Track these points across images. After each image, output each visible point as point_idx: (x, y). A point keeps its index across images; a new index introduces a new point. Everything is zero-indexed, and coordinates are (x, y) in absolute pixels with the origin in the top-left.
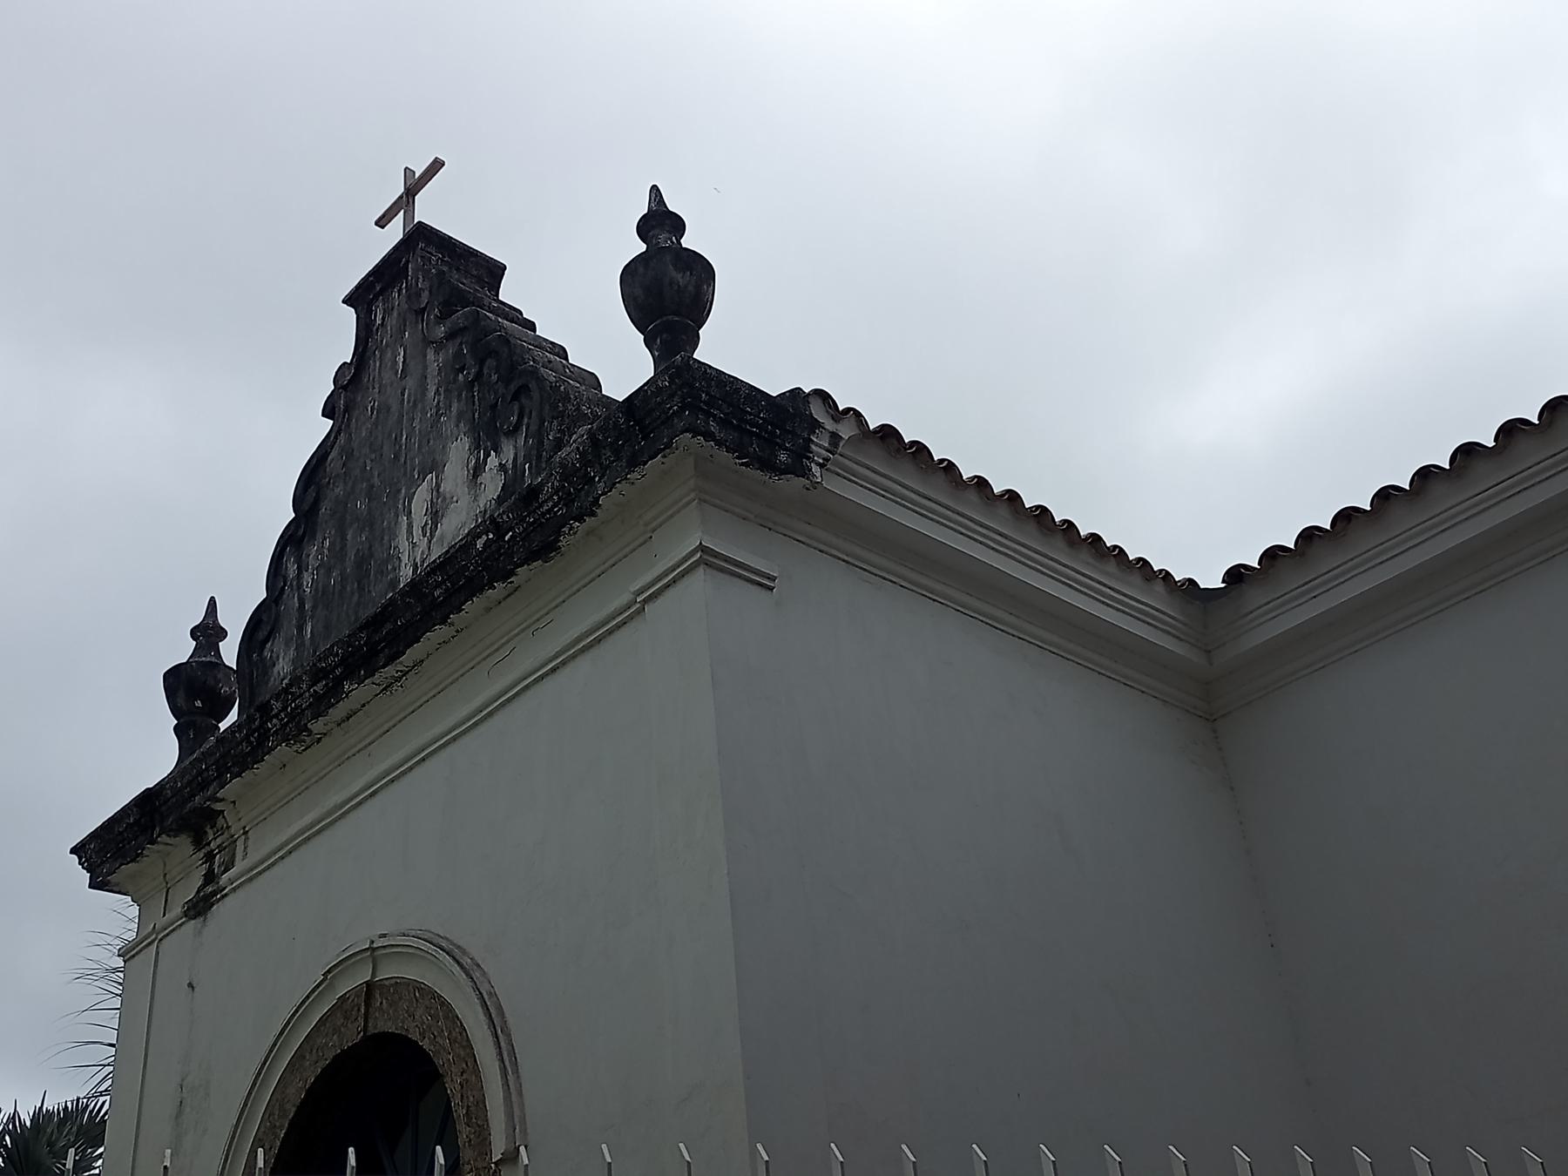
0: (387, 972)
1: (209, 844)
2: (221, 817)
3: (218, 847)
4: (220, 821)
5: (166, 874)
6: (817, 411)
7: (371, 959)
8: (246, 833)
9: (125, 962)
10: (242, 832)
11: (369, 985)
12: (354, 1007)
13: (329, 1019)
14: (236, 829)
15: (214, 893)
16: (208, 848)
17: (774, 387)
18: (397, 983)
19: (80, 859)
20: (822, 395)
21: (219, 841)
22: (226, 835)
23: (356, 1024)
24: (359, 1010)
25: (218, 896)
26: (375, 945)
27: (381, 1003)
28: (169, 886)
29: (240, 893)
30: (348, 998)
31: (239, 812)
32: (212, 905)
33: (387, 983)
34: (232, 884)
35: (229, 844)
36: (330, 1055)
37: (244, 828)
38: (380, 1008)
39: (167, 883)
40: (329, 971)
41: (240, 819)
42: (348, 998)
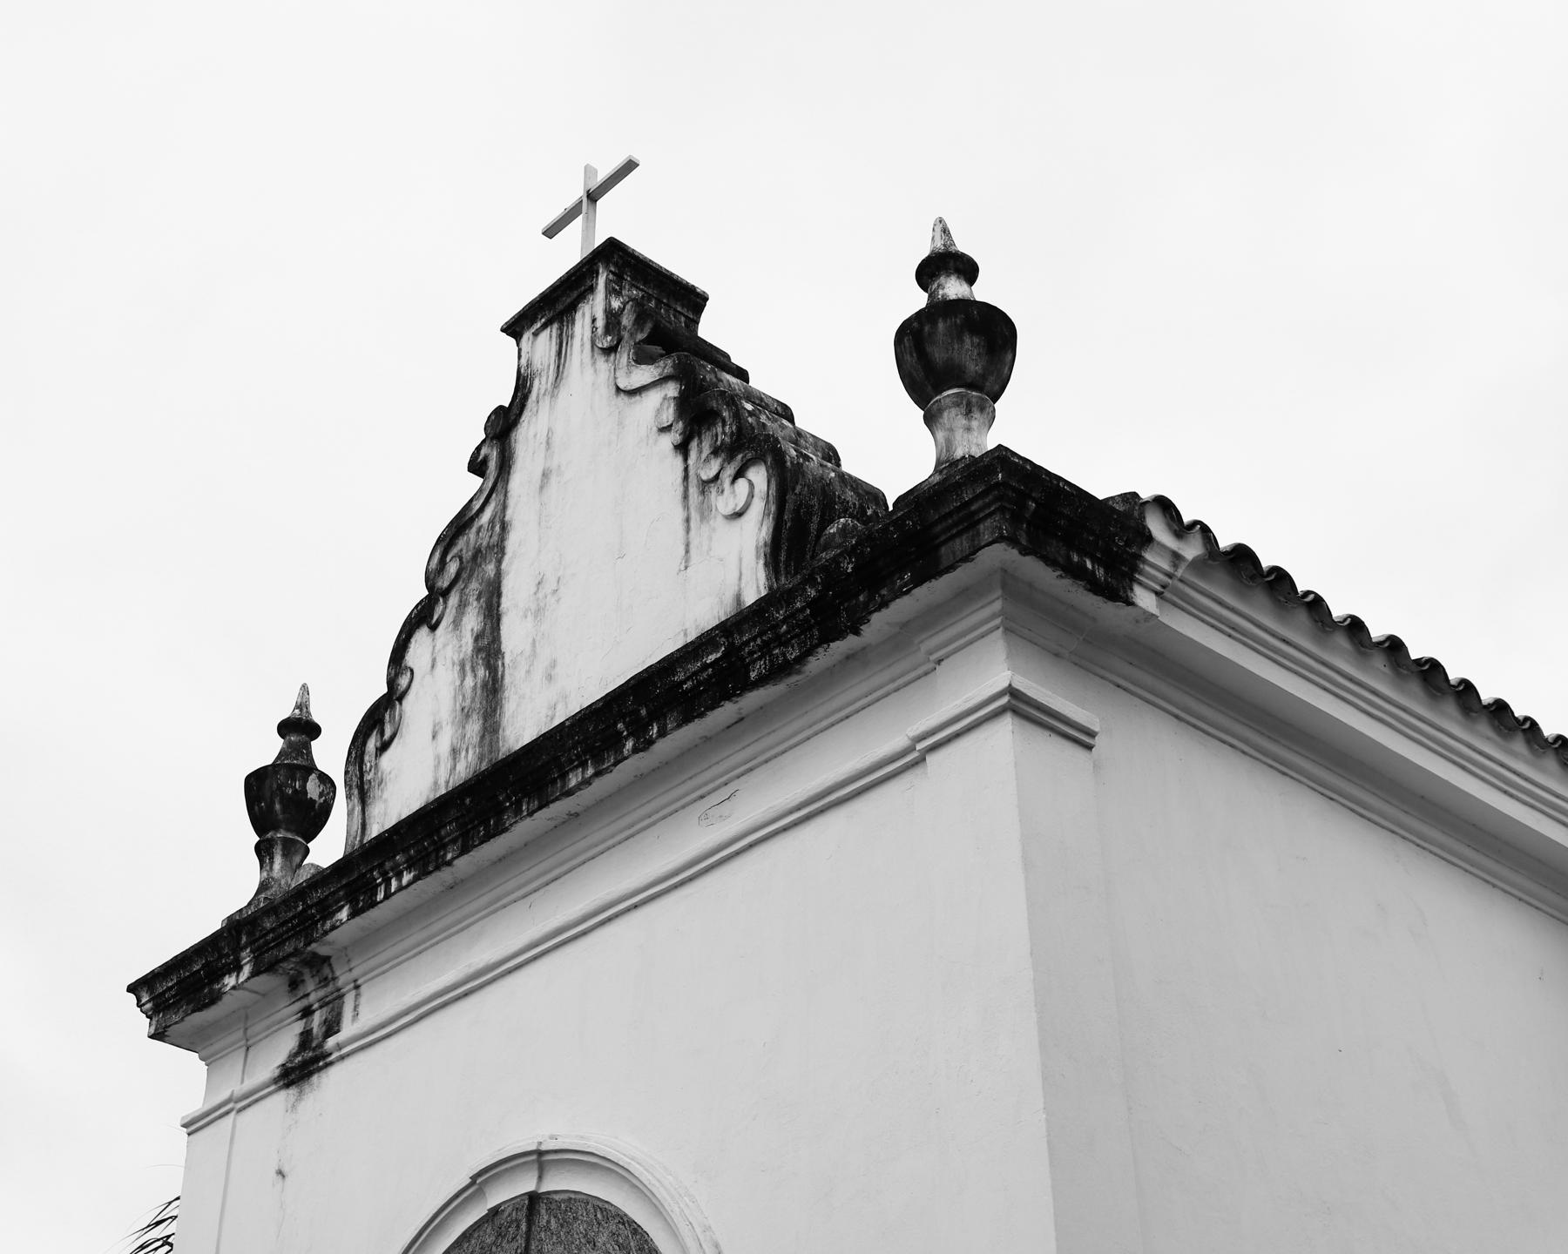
0: (558, 1182)
1: (307, 995)
2: (326, 965)
3: (319, 1001)
4: (326, 971)
5: (246, 1029)
6: (1156, 526)
8: (357, 987)
9: (189, 1134)
10: (352, 985)
11: (533, 1198)
12: (512, 1222)
13: (476, 1235)
14: (343, 979)
15: (316, 1060)
16: (304, 1003)
17: (1102, 487)
18: (571, 1199)
19: (139, 1000)
20: (1164, 505)
21: (321, 993)
22: (330, 988)
23: (515, 1245)
24: (518, 1227)
25: (321, 1064)
26: (543, 1148)
27: (548, 1222)
29: (348, 1063)
30: (503, 1211)
31: (349, 961)
32: (310, 1074)
33: (557, 1197)
34: (340, 1049)
35: (335, 999)
37: (355, 981)
38: (547, 1228)
39: (247, 1040)
40: (480, 1174)
41: (350, 970)
42: (503, 1211)
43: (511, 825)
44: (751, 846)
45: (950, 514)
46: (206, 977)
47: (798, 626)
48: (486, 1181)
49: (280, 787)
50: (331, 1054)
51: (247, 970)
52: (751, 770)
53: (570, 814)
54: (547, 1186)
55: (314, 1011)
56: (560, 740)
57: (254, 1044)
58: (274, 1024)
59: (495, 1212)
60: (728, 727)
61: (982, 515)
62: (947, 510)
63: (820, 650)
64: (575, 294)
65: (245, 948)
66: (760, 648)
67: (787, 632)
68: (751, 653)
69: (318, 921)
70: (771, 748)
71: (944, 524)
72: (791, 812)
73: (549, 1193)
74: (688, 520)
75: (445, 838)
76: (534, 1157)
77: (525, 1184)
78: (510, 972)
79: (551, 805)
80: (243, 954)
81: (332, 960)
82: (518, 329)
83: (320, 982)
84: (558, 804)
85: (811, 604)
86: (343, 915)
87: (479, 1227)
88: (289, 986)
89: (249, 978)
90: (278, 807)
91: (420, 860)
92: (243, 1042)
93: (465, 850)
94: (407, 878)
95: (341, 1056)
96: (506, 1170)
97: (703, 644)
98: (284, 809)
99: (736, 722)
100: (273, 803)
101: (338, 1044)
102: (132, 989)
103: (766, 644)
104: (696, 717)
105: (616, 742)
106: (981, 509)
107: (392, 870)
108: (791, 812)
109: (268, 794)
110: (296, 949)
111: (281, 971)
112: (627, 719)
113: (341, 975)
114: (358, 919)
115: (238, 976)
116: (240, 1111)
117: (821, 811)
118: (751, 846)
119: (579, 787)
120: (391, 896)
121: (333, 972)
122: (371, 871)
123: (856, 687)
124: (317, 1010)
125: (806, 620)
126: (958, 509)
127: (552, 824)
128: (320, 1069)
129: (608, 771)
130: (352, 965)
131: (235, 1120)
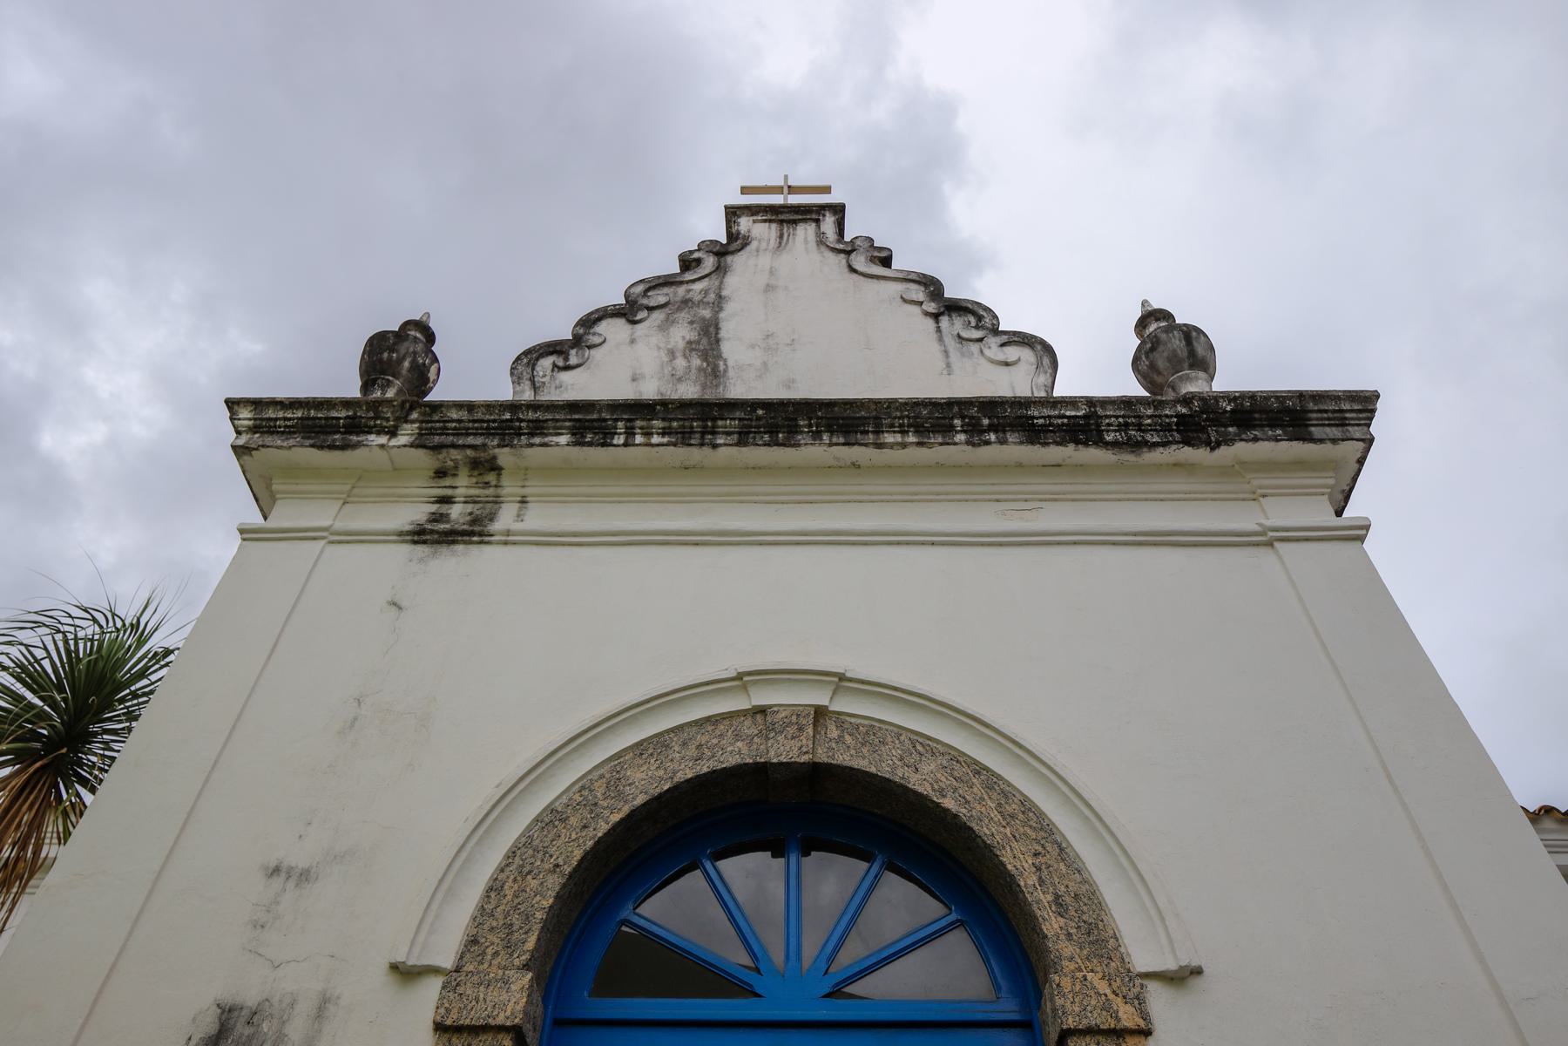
5: (353, 487)
7: (833, 687)
10: (519, 499)
11: (820, 713)
21: (473, 492)
22: (491, 491)
28: (351, 499)
31: (526, 479)
32: (454, 542)
34: (508, 535)
36: (731, 761)
39: (349, 496)
40: (750, 673)
43: (806, 444)
44: (1075, 543)
45: (1326, 411)
46: (344, 426)
47: (1161, 425)
48: (756, 682)
49: (415, 353)
50: (492, 535)
51: (402, 440)
52: (1056, 500)
53: (853, 464)
54: (834, 707)
55: (455, 503)
56: (886, 409)
57: (353, 502)
58: (393, 495)
59: (762, 711)
60: (1044, 466)
61: (1352, 422)
62: (1326, 408)
63: (1174, 447)
64: (800, 217)
65: (413, 422)
66: (1119, 425)
67: (1150, 425)
68: (1109, 425)
69: (524, 434)
70: (1084, 493)
71: (1319, 415)
72: (1126, 534)
73: (839, 713)
74: (946, 353)
75: (719, 427)
76: (836, 679)
77: (820, 697)
78: (761, 544)
79: (856, 448)
80: (408, 426)
81: (503, 471)
82: (738, 213)
83: (477, 483)
84: (863, 449)
85: (1179, 416)
86: (563, 439)
87: (730, 717)
88: (435, 473)
89: (405, 446)
90: (406, 364)
91: (680, 433)
92: (345, 496)
93: (741, 443)
94: (656, 439)
95: (506, 540)
96: (789, 679)
97: (1065, 402)
98: (411, 369)
99: (1053, 466)
100: (404, 358)
101: (508, 531)
102: (231, 404)
103: (1126, 425)
104: (1040, 443)
105: (948, 429)
106: (1352, 419)
107: (641, 428)
108: (1126, 534)
109: (403, 351)
110: (484, 445)
111: (440, 457)
112: (967, 420)
113: (507, 486)
114: (577, 449)
115: (389, 439)
116: (332, 542)
117: (1155, 544)
118: (1075, 543)
119: (892, 446)
120: (630, 445)
121: (498, 480)
122: (616, 420)
123: (1180, 484)
124: (459, 502)
125: (1169, 424)
126: (1334, 411)
127: (835, 463)
128: (465, 543)
129: (930, 446)
130: (527, 483)
131: (324, 547)
